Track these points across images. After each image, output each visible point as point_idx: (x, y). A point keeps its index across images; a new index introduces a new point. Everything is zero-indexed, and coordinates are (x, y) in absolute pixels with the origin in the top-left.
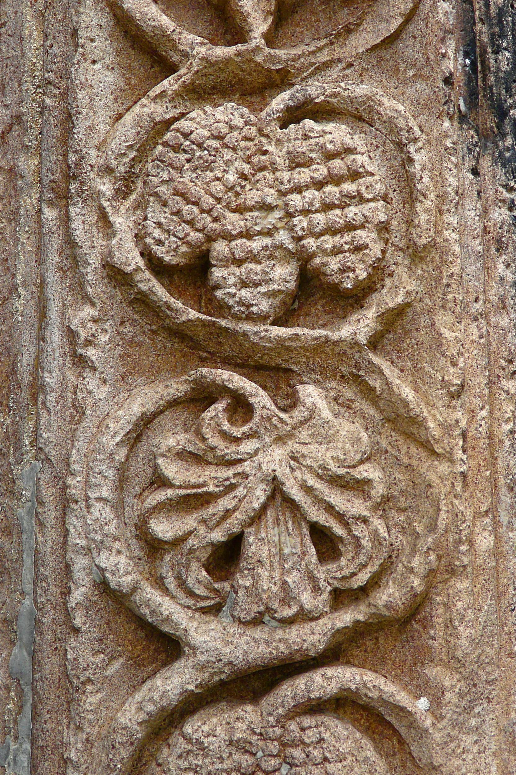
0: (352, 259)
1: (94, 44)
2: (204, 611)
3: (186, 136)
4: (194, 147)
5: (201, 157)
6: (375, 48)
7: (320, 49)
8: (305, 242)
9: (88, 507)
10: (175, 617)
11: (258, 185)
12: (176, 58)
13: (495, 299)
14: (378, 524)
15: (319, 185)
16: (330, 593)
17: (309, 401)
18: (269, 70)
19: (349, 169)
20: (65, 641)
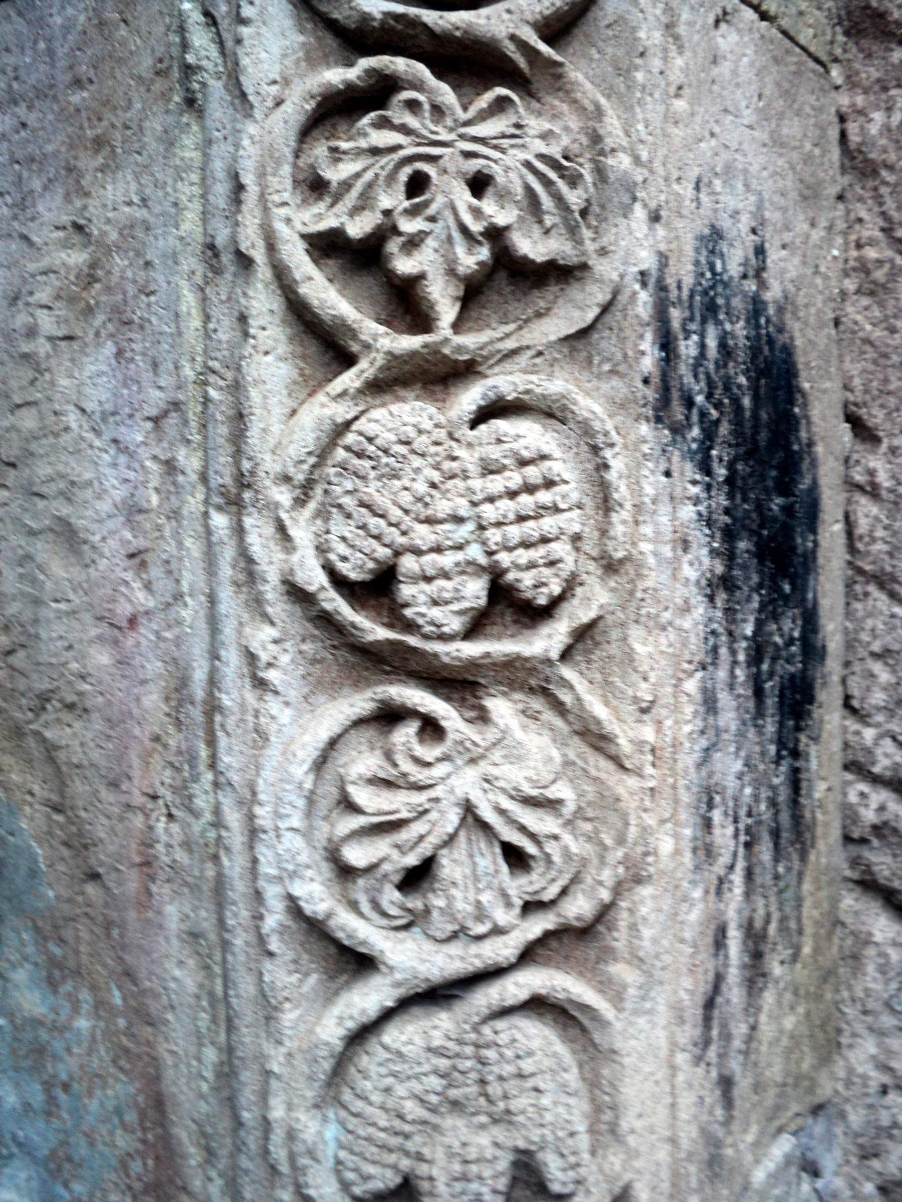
0: (546, 571)
1: (266, 333)
2: (397, 929)
3: (370, 440)
4: (380, 453)
5: (387, 465)
6: (568, 338)
7: (508, 336)
8: (497, 557)
11: (449, 495)
12: (355, 348)
14: (567, 838)
15: (512, 494)
17: (501, 722)
18: (456, 361)
19: (545, 478)
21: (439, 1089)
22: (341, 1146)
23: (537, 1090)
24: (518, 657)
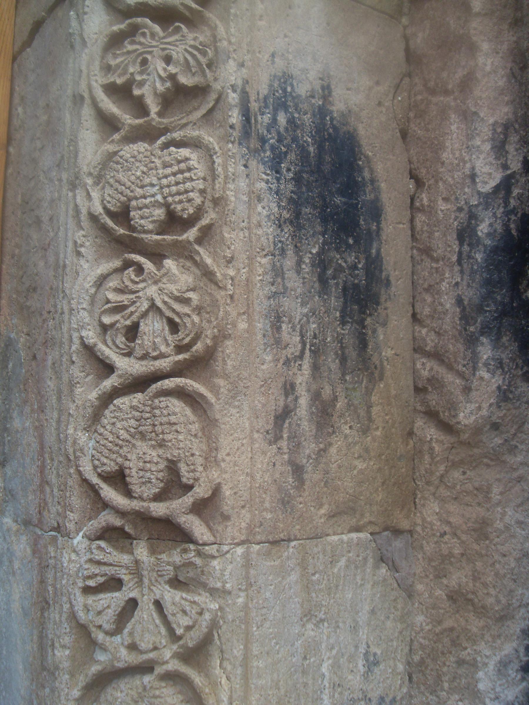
2: (124, 355)
3: (121, 157)
9: (78, 312)
10: (110, 356)
12: (120, 126)
13: (255, 222)
15: (174, 174)
16: (174, 346)
17: (167, 266)
18: (159, 128)
20: (70, 368)
21: (135, 426)
22: (94, 449)
23: (177, 431)
24: (177, 240)
